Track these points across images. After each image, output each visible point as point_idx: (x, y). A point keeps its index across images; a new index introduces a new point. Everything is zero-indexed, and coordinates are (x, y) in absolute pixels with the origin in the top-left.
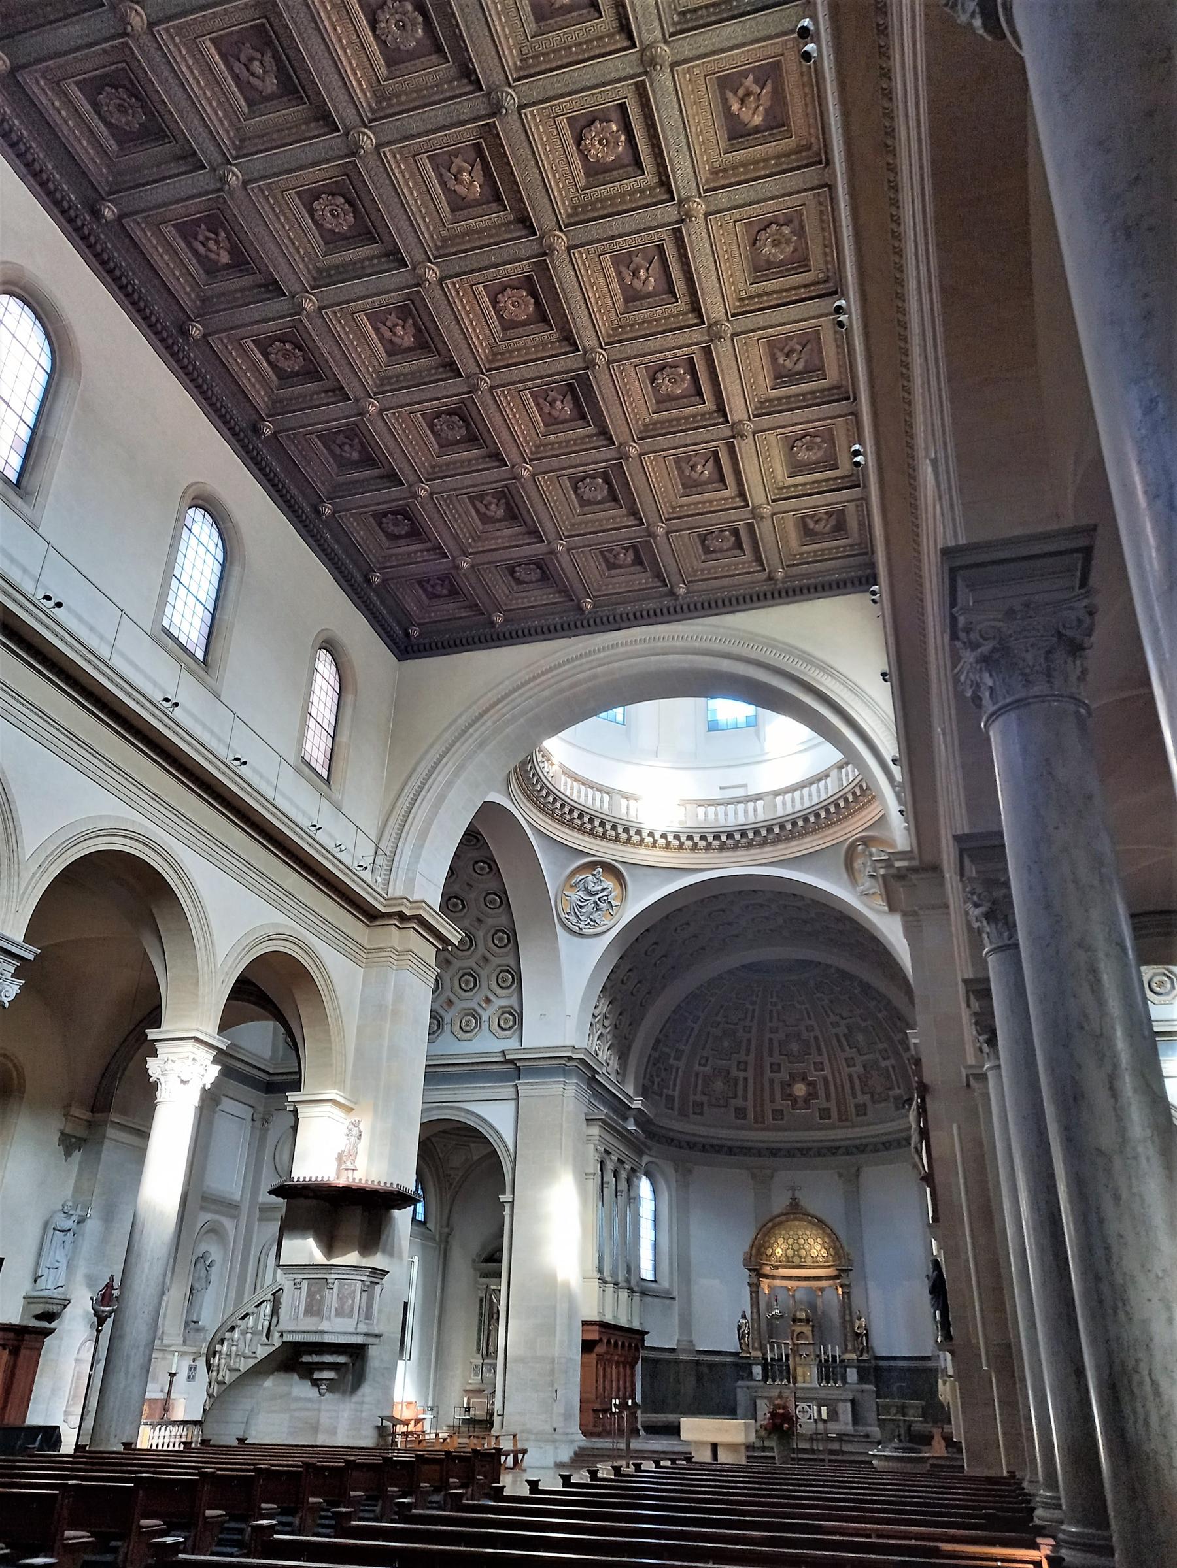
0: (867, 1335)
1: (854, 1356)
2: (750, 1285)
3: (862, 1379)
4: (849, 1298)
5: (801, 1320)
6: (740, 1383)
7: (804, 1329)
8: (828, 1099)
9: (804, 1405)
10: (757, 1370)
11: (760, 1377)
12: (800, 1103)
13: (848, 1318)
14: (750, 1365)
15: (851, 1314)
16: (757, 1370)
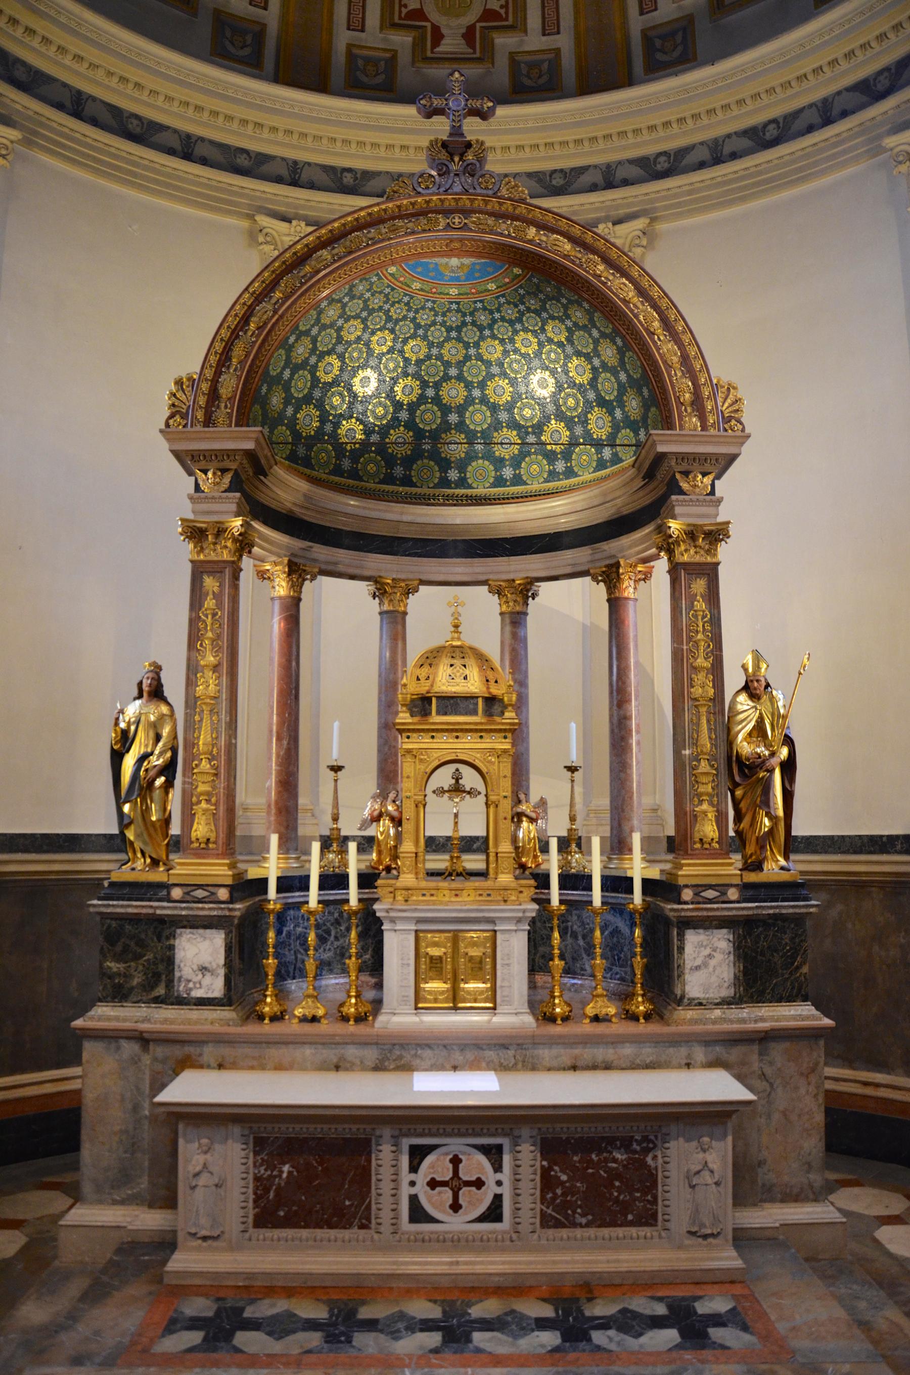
0: (789, 768)
1: (731, 867)
2: (195, 533)
3: (757, 978)
4: (713, 596)
5: (452, 703)
6: (105, 1015)
7: (468, 745)
8: (550, 27)
9: (456, 1145)
10: (200, 956)
11: (214, 986)
12: (451, 44)
13: (703, 688)
14: (165, 928)
15: (717, 670)
16: (200, 956)
